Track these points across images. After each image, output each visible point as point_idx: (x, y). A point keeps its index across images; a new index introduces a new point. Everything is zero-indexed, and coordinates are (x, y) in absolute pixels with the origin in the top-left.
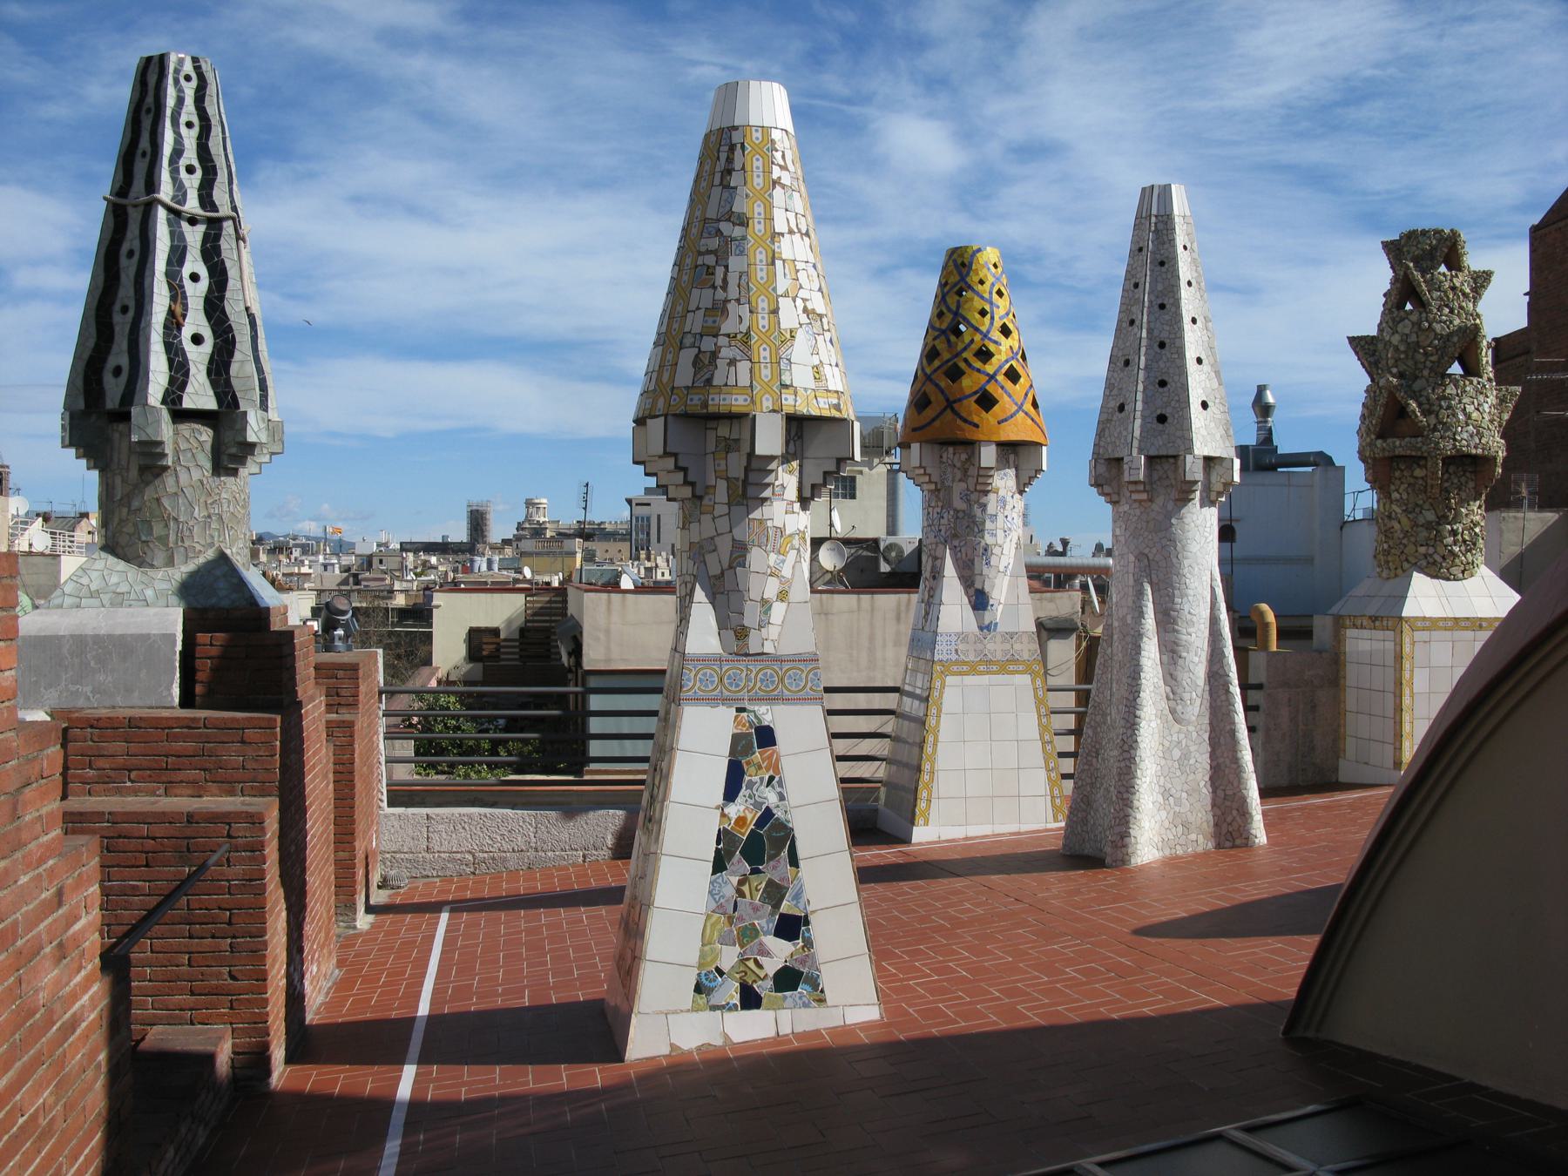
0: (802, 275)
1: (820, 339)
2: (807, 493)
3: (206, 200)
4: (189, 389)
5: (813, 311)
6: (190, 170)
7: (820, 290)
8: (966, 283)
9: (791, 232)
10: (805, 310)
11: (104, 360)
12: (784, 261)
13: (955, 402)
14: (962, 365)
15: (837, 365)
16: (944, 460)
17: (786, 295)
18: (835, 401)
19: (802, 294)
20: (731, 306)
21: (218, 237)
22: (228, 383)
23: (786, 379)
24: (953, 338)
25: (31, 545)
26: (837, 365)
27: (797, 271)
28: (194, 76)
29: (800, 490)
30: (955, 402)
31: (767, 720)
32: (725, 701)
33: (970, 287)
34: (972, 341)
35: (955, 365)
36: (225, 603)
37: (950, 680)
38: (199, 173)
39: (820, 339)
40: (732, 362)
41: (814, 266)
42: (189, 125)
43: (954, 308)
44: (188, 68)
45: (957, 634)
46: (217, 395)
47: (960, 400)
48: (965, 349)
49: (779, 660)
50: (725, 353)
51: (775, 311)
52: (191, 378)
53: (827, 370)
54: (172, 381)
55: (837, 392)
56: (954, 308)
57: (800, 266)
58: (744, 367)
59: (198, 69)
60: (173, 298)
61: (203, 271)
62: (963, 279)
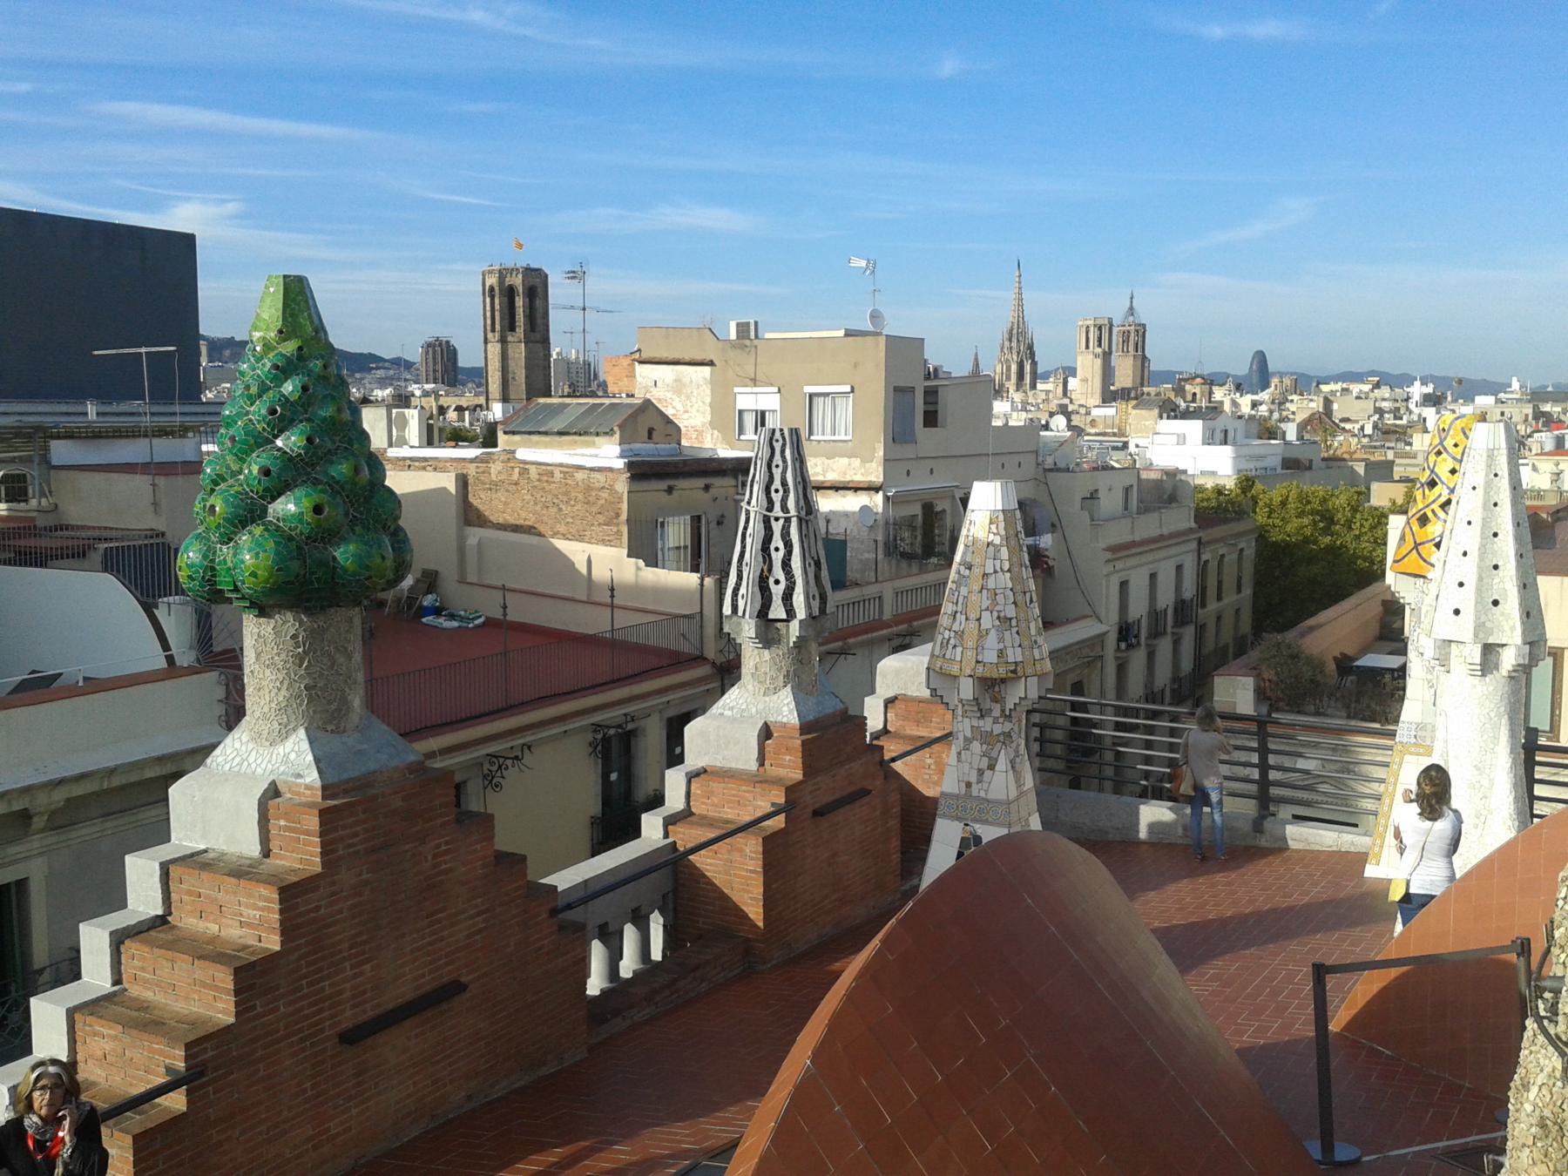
0: (1000, 598)
1: (1007, 634)
2: (1007, 713)
3: (785, 509)
4: (772, 608)
5: (1005, 617)
6: (777, 491)
7: (1015, 603)
8: (1443, 447)
9: (995, 572)
10: (999, 618)
11: (738, 590)
12: (988, 590)
13: (1420, 544)
14: (1430, 515)
15: (1020, 646)
16: (1417, 586)
17: (987, 609)
18: (1013, 668)
19: (998, 608)
20: (958, 615)
21: (789, 526)
22: (792, 605)
23: (980, 659)
24: (1427, 491)
25: (973, 511)
26: (1020, 646)
27: (996, 594)
28: (780, 439)
29: (1003, 711)
30: (1420, 544)
31: (979, 832)
32: (958, 819)
33: (1445, 449)
34: (1440, 495)
35: (1425, 513)
36: (785, 720)
37: (1407, 758)
38: (781, 492)
39: (1007, 634)
40: (955, 646)
41: (1011, 590)
42: (777, 466)
43: (1431, 467)
44: (778, 435)
45: (1418, 724)
46: (786, 611)
47: (1423, 543)
48: (1434, 501)
49: (988, 801)
50: (952, 641)
51: (979, 620)
52: (773, 603)
53: (1010, 651)
54: (763, 605)
55: (1016, 663)
56: (1431, 467)
57: (998, 591)
58: (959, 649)
59: (782, 435)
60: (764, 563)
61: (781, 545)
62: (1441, 443)
